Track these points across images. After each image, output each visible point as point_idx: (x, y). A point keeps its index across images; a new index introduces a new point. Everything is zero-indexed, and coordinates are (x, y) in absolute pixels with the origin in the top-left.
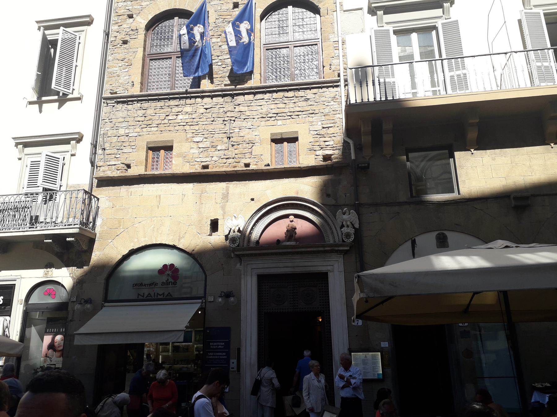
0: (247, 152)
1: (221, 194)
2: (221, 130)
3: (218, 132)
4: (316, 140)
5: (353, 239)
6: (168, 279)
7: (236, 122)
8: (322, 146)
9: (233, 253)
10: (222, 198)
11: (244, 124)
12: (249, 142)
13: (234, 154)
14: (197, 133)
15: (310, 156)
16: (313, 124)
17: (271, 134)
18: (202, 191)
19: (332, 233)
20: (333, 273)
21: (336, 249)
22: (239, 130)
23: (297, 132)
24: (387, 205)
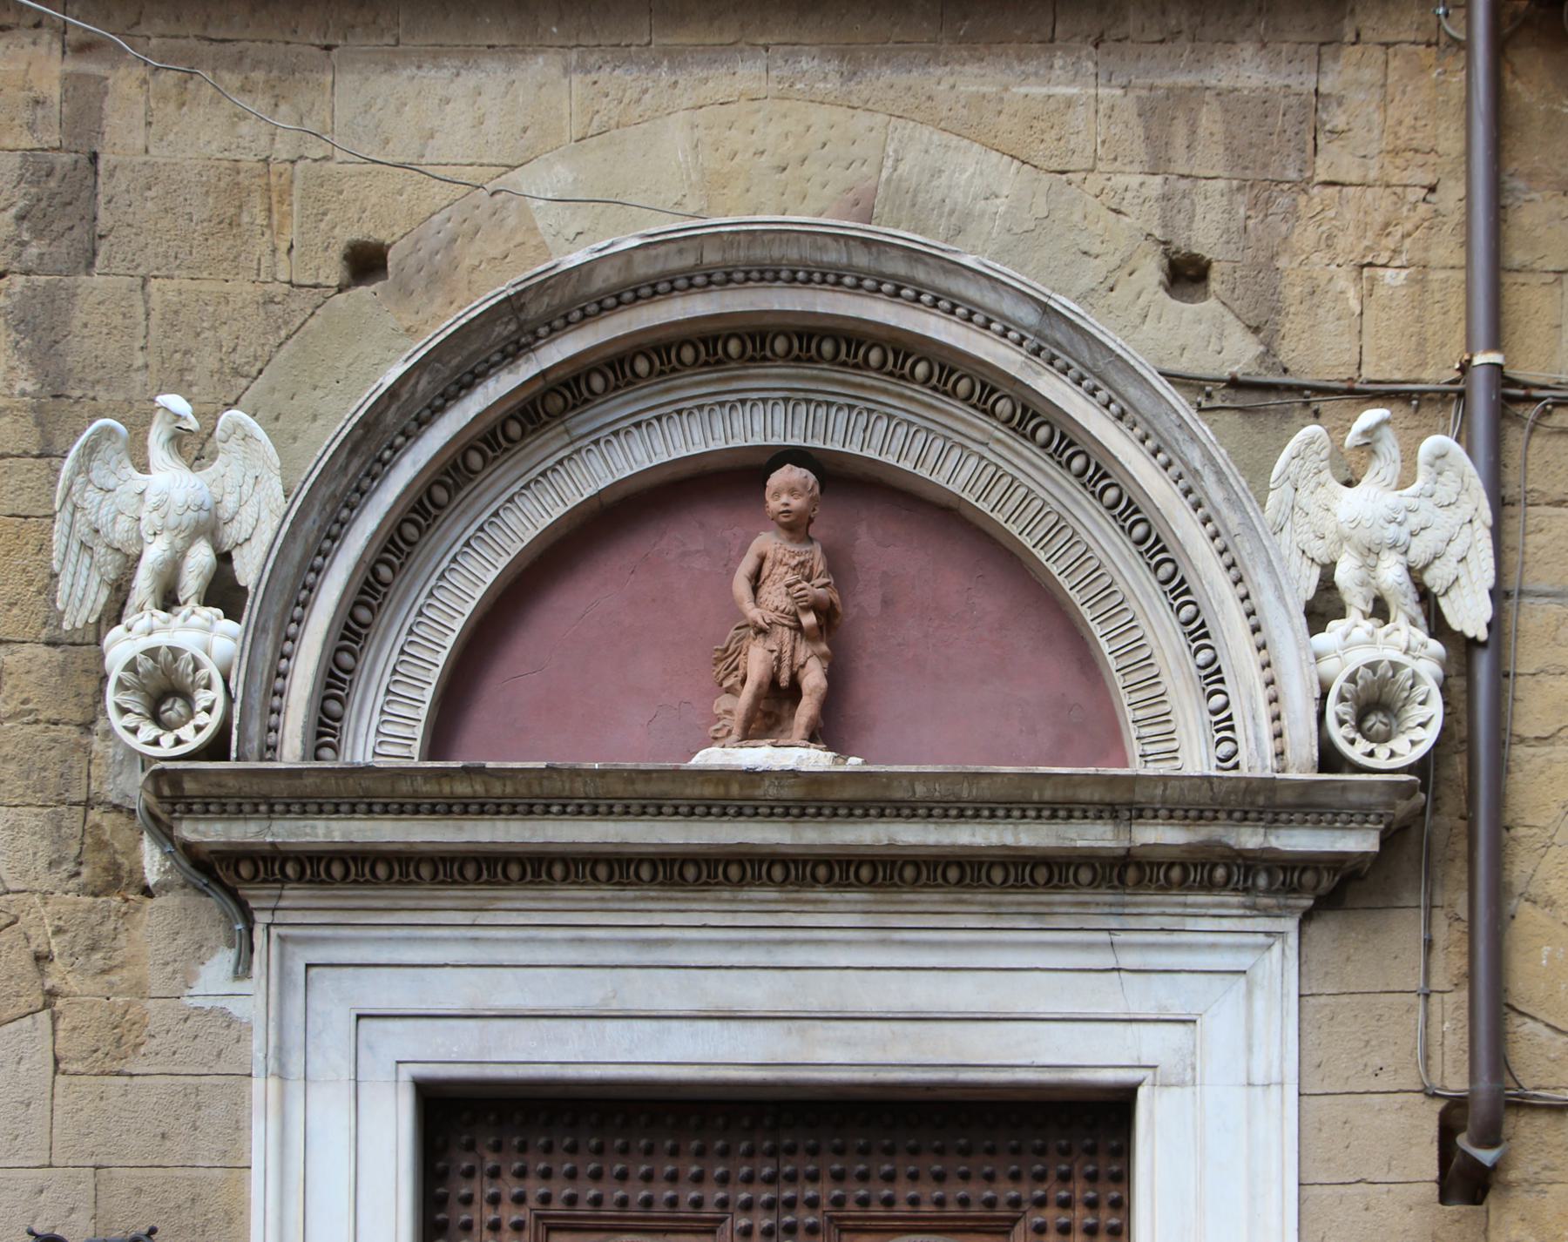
1: (15, 159)
5: (1430, 736)
9: (162, 830)
10: (21, 218)
19: (1212, 676)
20: (1188, 1090)
21: (1250, 839)
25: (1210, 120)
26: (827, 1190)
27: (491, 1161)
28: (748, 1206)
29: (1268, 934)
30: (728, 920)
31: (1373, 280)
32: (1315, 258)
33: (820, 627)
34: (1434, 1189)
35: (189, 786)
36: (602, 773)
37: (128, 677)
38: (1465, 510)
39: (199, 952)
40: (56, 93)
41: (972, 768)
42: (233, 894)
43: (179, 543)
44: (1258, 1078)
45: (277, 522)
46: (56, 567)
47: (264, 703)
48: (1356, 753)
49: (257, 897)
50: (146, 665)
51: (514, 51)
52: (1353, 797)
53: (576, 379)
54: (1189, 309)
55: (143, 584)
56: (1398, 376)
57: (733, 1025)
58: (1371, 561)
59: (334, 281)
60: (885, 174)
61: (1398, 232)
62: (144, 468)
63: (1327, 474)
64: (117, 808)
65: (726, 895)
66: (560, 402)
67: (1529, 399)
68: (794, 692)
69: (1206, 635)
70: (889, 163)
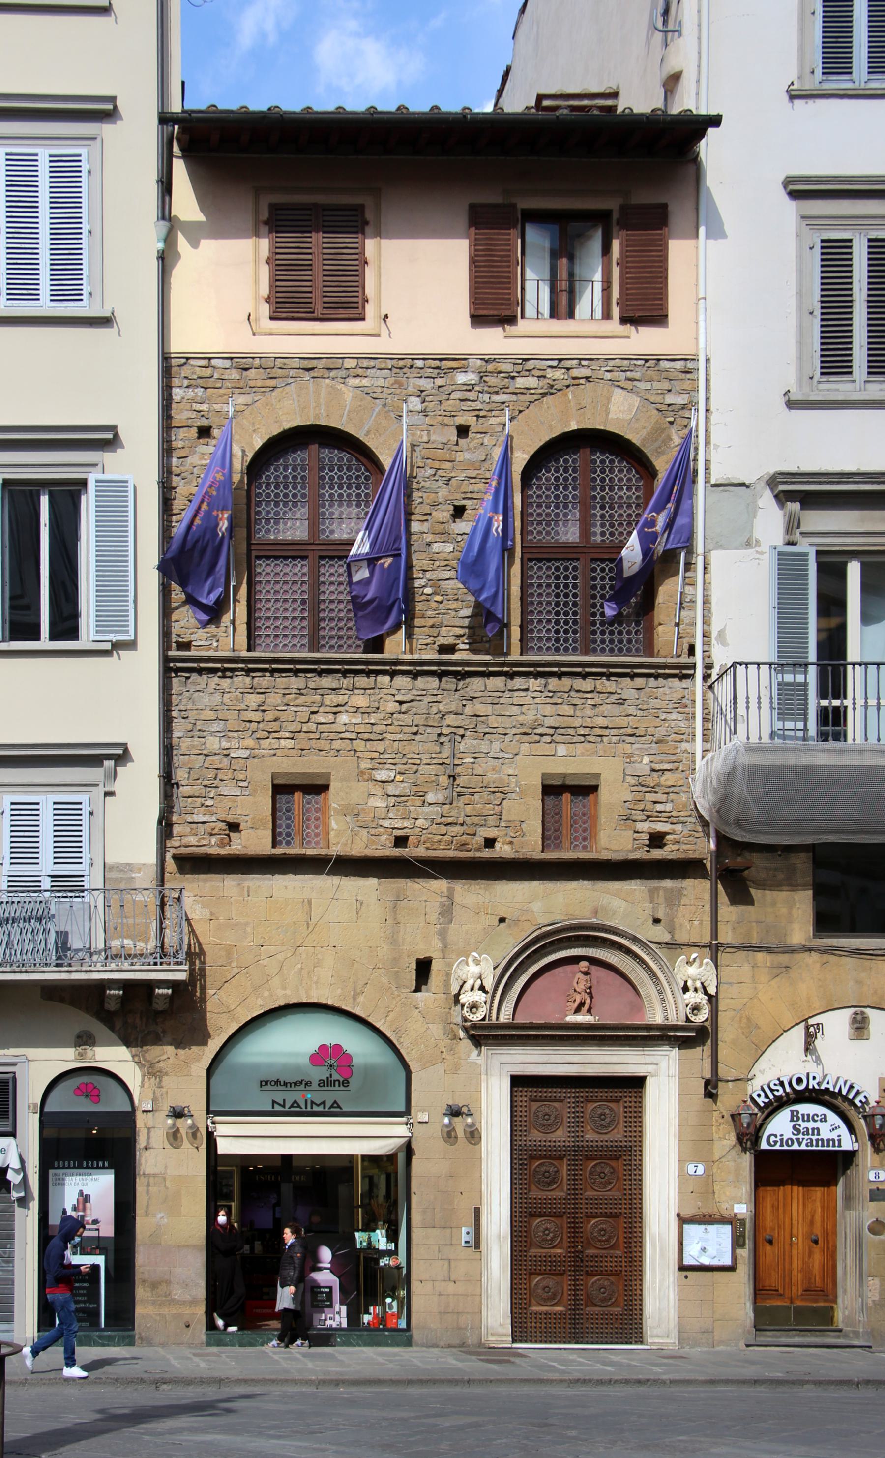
0: (492, 812)
2: (434, 755)
3: (428, 761)
4: (639, 796)
6: (331, 1075)
7: (466, 740)
8: (649, 813)
11: (484, 746)
12: (496, 790)
13: (463, 814)
14: (382, 761)
15: (624, 833)
16: (632, 759)
17: (543, 775)
18: (398, 896)
22: (472, 760)
23: (598, 776)
24: (768, 950)
68: (584, 1003)
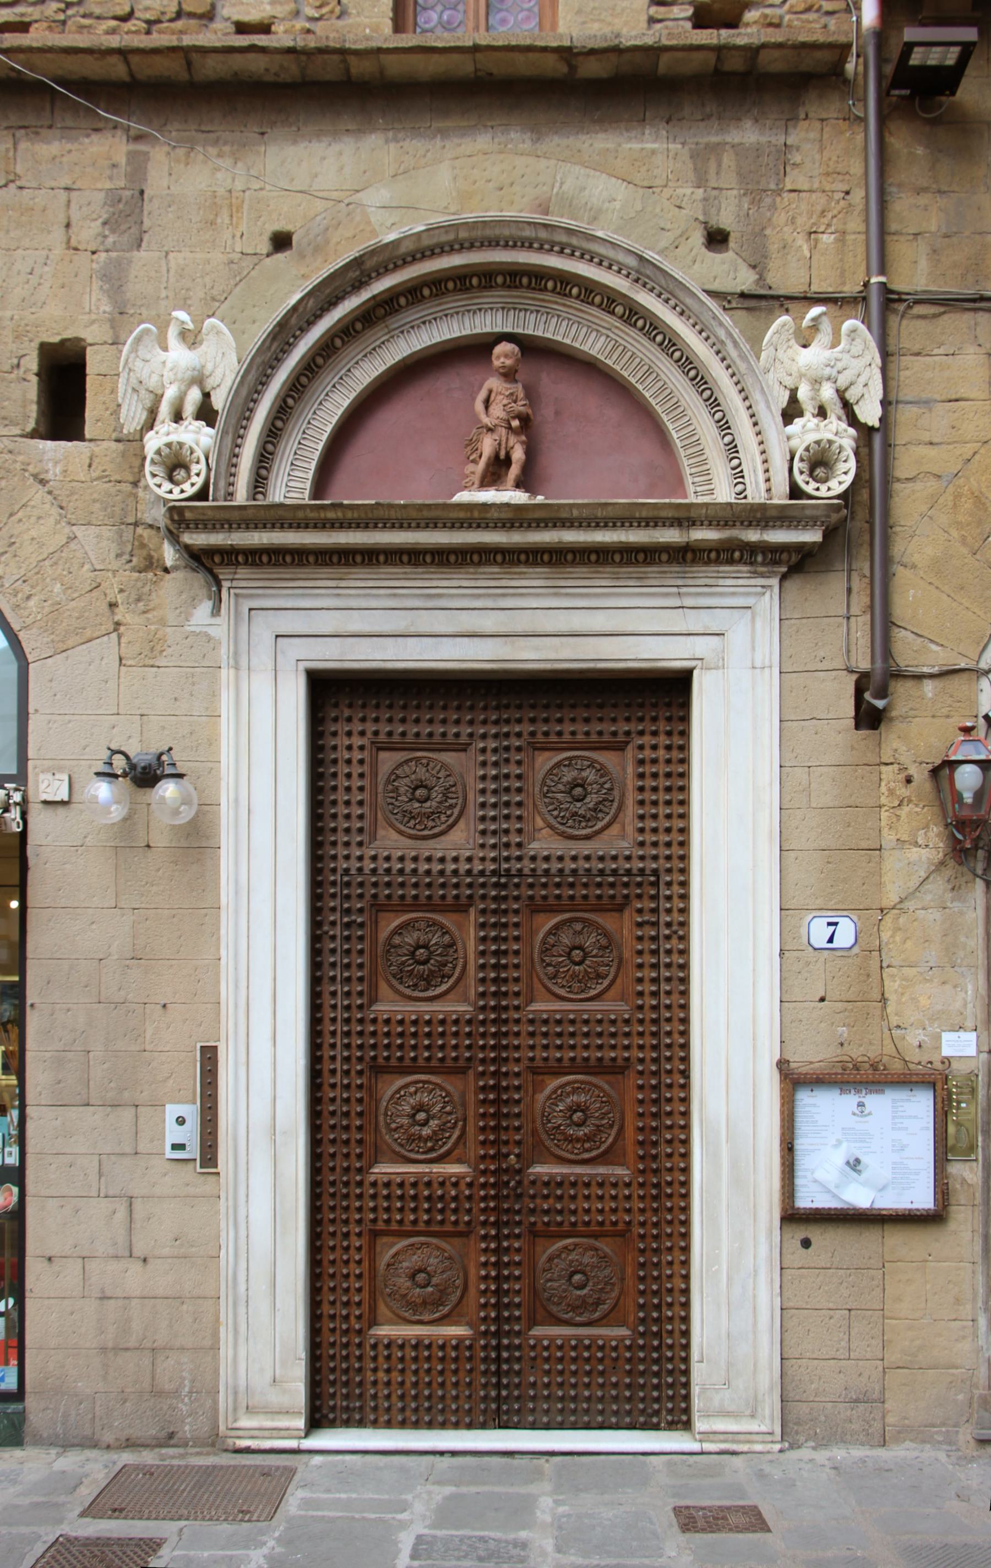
1: (102, 195)
5: (849, 479)
9: (174, 538)
10: (105, 223)
19: (732, 449)
20: (721, 671)
21: (753, 536)
25: (728, 159)
26: (527, 728)
27: (347, 713)
28: (484, 736)
29: (763, 587)
30: (473, 583)
31: (816, 241)
32: (785, 229)
33: (521, 427)
34: (852, 722)
35: (188, 515)
36: (405, 506)
37: (157, 458)
38: (867, 359)
39: (193, 602)
40: (123, 161)
41: (603, 501)
42: (210, 571)
43: (183, 388)
44: (758, 664)
45: (233, 376)
46: (120, 400)
47: (227, 470)
48: (810, 488)
49: (223, 573)
50: (166, 451)
51: (360, 132)
52: (808, 512)
53: (391, 300)
54: (718, 257)
55: (165, 410)
56: (830, 290)
57: (475, 639)
58: (817, 386)
59: (265, 251)
60: (555, 190)
61: (830, 215)
62: (165, 349)
63: (793, 342)
64: (151, 526)
65: (471, 570)
66: (383, 311)
67: (901, 300)
68: (508, 462)
69: (729, 428)
70: (557, 185)
